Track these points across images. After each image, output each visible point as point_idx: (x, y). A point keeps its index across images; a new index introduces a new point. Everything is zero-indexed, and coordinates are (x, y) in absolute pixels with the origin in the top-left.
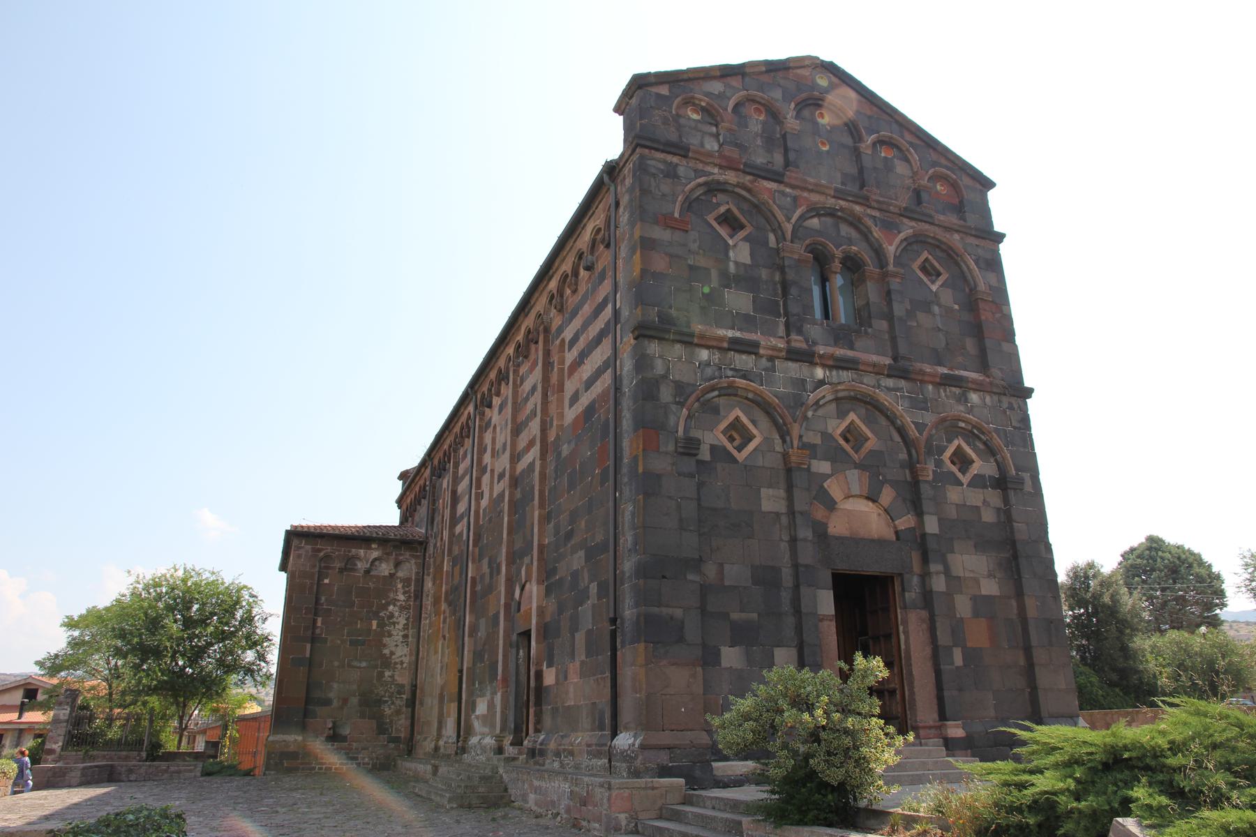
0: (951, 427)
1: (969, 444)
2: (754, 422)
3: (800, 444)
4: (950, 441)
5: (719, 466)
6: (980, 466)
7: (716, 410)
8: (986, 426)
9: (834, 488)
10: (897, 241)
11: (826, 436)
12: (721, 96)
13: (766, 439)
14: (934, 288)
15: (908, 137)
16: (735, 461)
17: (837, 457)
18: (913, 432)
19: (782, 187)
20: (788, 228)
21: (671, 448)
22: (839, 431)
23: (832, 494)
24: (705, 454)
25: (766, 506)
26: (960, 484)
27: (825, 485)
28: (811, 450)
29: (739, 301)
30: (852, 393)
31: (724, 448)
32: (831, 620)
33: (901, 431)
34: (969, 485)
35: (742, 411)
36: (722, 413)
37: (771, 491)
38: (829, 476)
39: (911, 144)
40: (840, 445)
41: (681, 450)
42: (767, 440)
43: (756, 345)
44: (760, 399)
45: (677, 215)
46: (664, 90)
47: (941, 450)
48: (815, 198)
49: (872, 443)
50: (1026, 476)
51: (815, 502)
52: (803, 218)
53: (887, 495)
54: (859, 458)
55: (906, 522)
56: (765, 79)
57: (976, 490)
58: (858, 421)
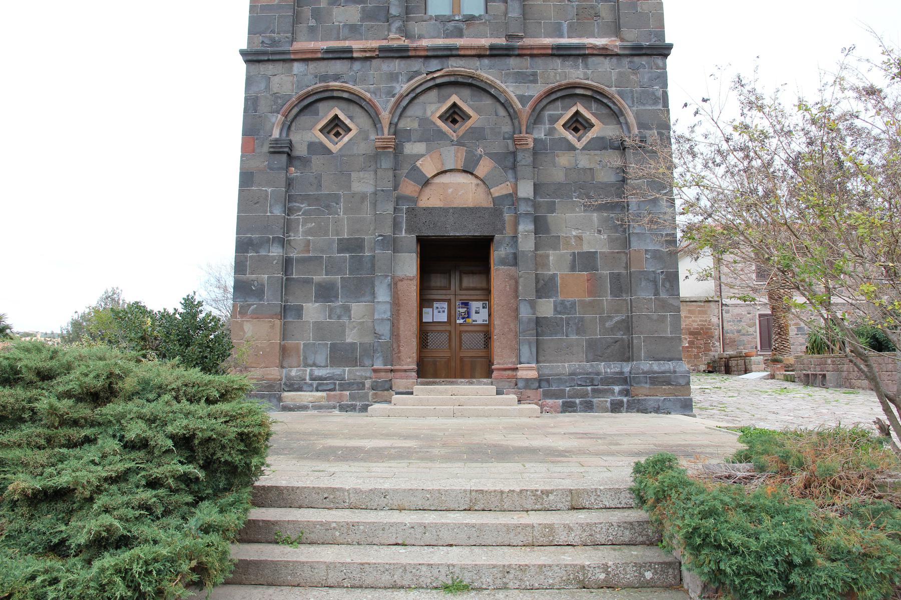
1: (588, 108)
2: (351, 118)
3: (392, 130)
5: (314, 158)
6: (600, 129)
8: (606, 88)
9: (428, 167)
11: (424, 121)
13: (361, 131)
16: (329, 152)
17: (432, 137)
21: (266, 149)
22: (438, 114)
23: (425, 172)
24: (301, 150)
26: (572, 148)
27: (418, 164)
30: (452, 79)
31: (321, 143)
32: (411, 280)
33: (506, 105)
34: (584, 149)
35: (341, 110)
36: (321, 114)
37: (361, 174)
38: (423, 156)
40: (438, 127)
41: (272, 150)
42: (363, 135)
43: (350, 50)
44: (355, 96)
47: (554, 120)
50: (653, 135)
51: (407, 180)
53: (484, 167)
54: (457, 136)
55: (499, 190)
57: (592, 152)
58: (460, 103)
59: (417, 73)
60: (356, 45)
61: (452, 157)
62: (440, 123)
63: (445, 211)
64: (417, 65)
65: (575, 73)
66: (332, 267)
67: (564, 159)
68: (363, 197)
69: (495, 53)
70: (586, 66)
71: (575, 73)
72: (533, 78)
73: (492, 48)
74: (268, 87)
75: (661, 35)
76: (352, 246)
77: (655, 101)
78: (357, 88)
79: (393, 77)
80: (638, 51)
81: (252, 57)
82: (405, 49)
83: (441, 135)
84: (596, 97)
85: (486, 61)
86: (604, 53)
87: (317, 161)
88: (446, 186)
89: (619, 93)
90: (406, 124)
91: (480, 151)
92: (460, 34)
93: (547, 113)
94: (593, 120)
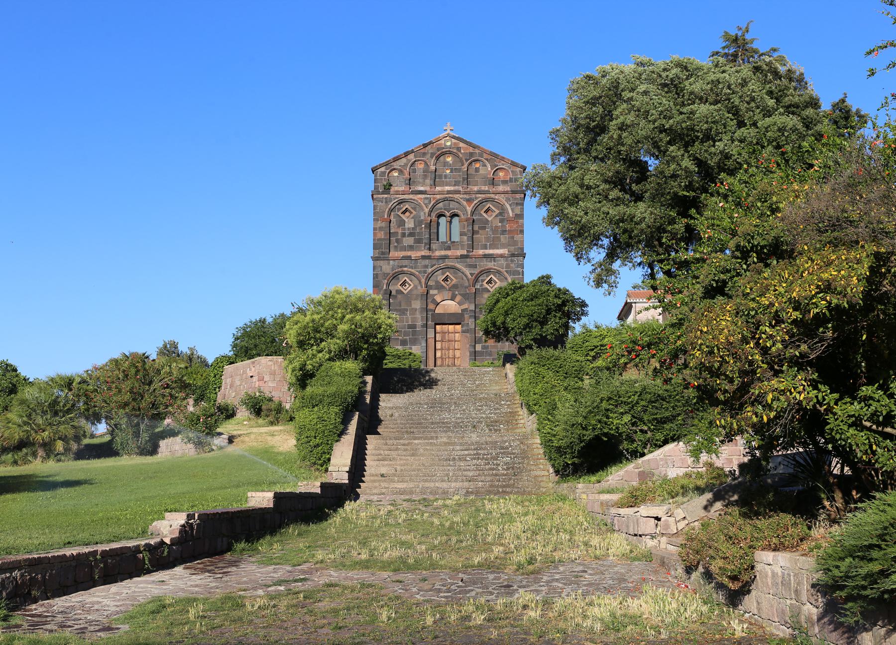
0: (488, 271)
1: (495, 276)
4: (487, 276)
7: (398, 279)
9: (438, 299)
10: (473, 204)
11: (437, 282)
12: (406, 165)
14: (490, 219)
15: (485, 156)
17: (440, 288)
18: (470, 276)
19: (426, 196)
20: (427, 210)
24: (394, 293)
25: (413, 306)
28: (431, 287)
29: (408, 241)
39: (487, 159)
42: (415, 287)
45: (386, 217)
46: (383, 169)
47: (483, 281)
48: (438, 197)
49: (455, 281)
52: (434, 206)
53: (458, 298)
56: (422, 151)
59: (434, 265)
60: (414, 254)
61: (448, 294)
62: (442, 283)
63: (444, 314)
64: (434, 262)
65: (491, 265)
66: (406, 334)
67: (486, 295)
68: (416, 310)
69: (463, 257)
70: (495, 262)
71: (491, 265)
72: (475, 266)
73: (461, 255)
74: (381, 270)
75: (522, 249)
76: (413, 327)
77: (519, 274)
78: (413, 271)
79: (426, 267)
80: (513, 255)
81: (375, 259)
82: (430, 256)
83: (443, 287)
84: (499, 272)
85: (459, 260)
86: (502, 256)
87: (399, 296)
88: (444, 305)
89: (506, 271)
90: (431, 283)
91: (457, 293)
92: (449, 248)
93: (480, 278)
94: (497, 281)
